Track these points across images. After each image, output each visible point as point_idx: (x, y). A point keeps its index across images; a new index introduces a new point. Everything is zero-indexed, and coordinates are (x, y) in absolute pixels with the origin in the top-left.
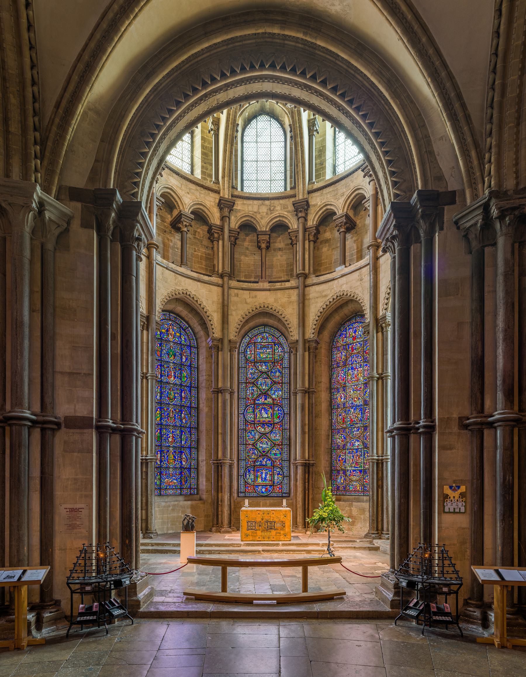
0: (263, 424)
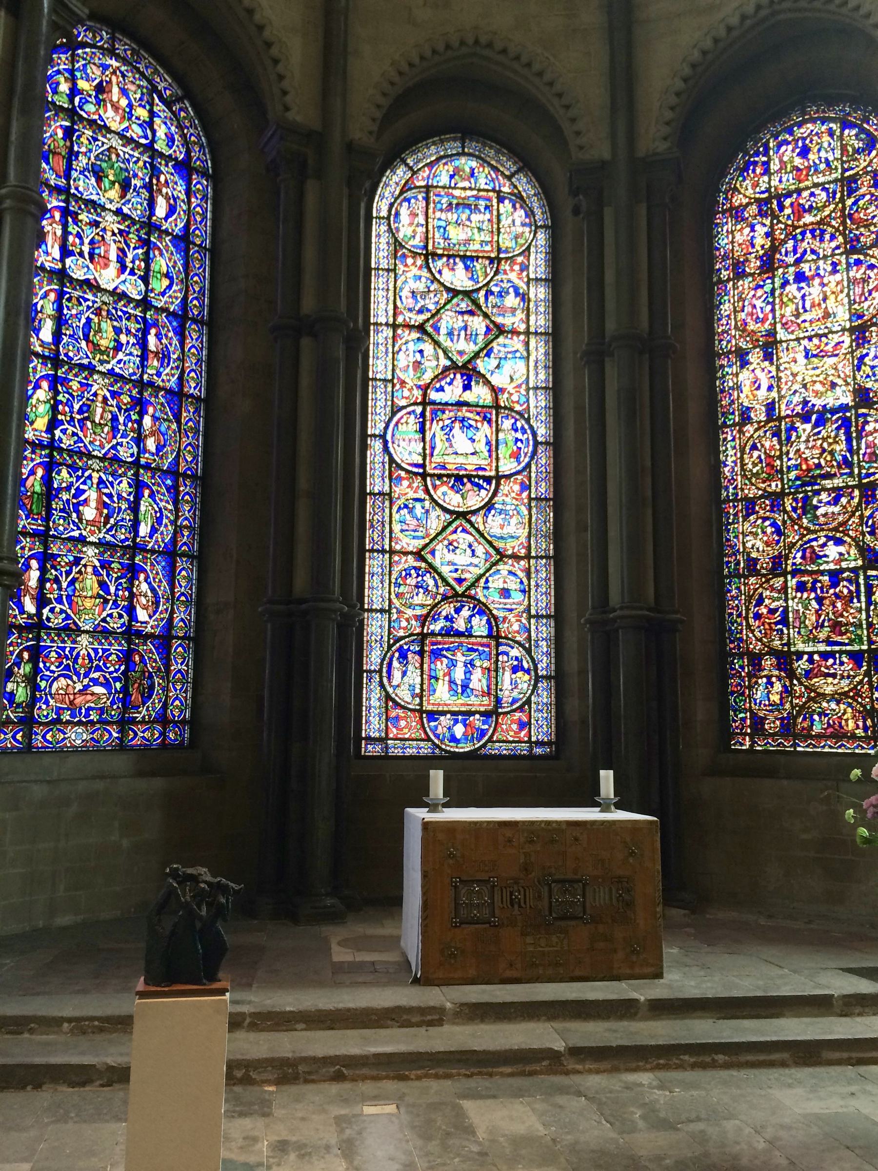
0: (459, 480)
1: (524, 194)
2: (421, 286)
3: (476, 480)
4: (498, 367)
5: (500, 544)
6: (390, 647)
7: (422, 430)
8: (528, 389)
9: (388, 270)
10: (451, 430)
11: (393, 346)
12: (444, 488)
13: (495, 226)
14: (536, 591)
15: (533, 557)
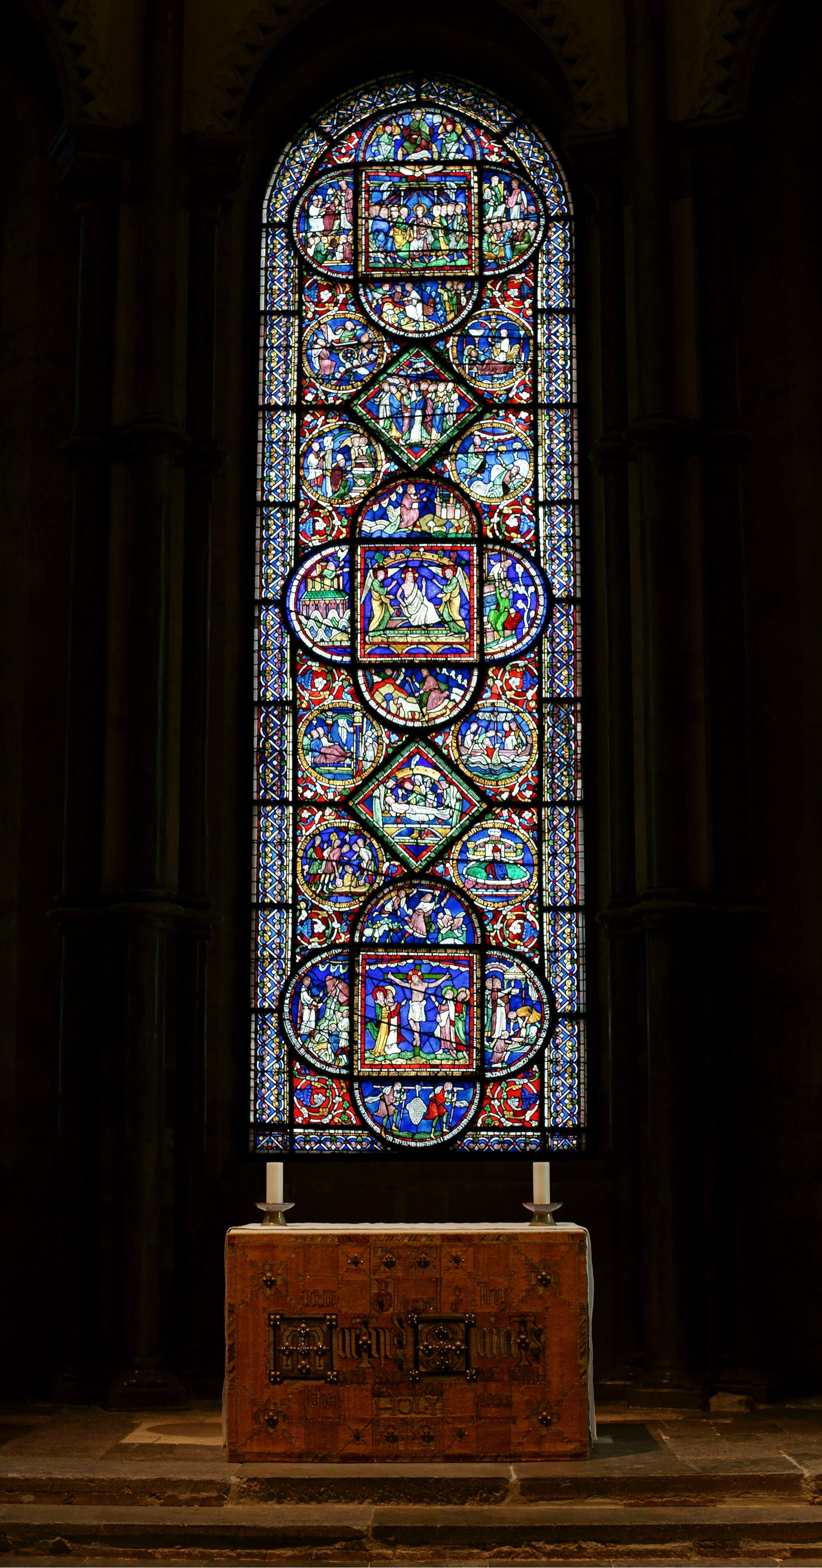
1: (526, 164)
2: (343, 336)
3: (444, 671)
4: (482, 469)
5: (489, 785)
6: (295, 967)
7: (349, 590)
8: (535, 506)
9: (287, 314)
10: (399, 585)
11: (298, 445)
12: (387, 689)
13: (475, 223)
14: (552, 864)
15: (547, 804)
